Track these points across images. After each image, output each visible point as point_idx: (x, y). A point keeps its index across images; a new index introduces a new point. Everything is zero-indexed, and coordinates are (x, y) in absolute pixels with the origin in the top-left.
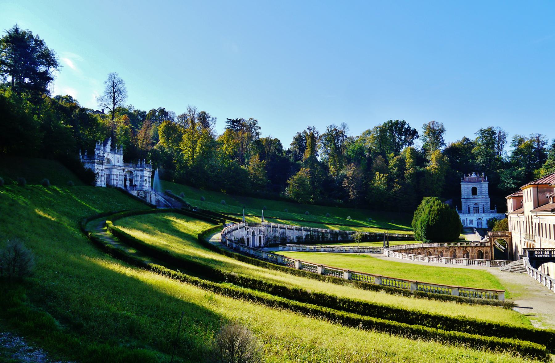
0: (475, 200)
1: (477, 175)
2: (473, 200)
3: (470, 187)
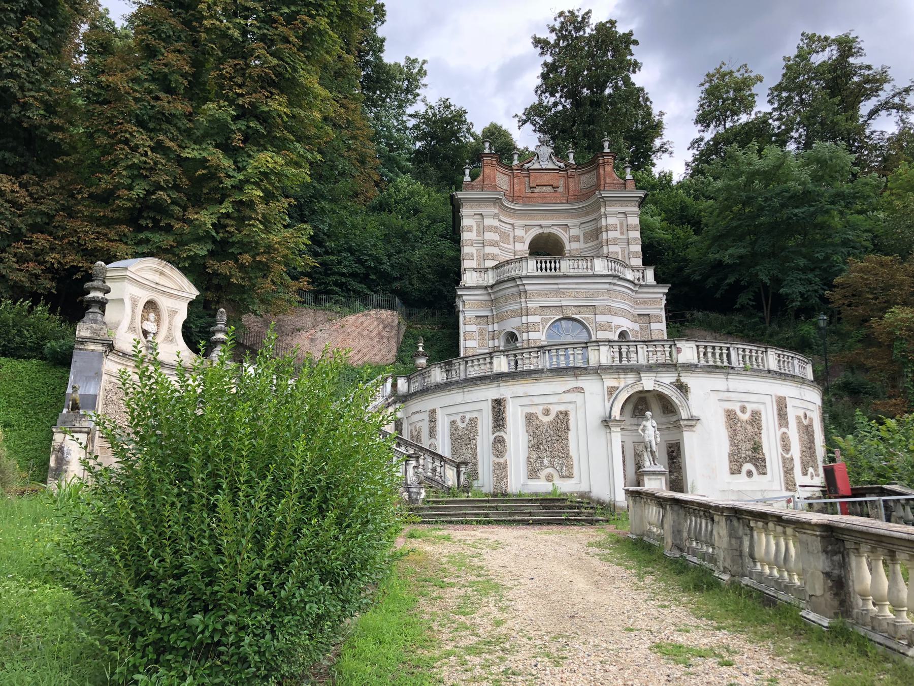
0: (560, 293)
1: (564, 158)
2: (546, 296)
3: (519, 232)
